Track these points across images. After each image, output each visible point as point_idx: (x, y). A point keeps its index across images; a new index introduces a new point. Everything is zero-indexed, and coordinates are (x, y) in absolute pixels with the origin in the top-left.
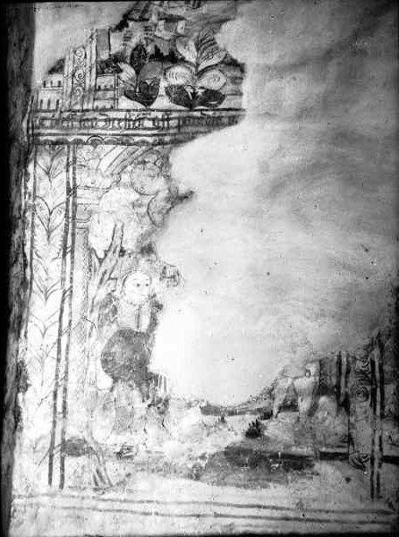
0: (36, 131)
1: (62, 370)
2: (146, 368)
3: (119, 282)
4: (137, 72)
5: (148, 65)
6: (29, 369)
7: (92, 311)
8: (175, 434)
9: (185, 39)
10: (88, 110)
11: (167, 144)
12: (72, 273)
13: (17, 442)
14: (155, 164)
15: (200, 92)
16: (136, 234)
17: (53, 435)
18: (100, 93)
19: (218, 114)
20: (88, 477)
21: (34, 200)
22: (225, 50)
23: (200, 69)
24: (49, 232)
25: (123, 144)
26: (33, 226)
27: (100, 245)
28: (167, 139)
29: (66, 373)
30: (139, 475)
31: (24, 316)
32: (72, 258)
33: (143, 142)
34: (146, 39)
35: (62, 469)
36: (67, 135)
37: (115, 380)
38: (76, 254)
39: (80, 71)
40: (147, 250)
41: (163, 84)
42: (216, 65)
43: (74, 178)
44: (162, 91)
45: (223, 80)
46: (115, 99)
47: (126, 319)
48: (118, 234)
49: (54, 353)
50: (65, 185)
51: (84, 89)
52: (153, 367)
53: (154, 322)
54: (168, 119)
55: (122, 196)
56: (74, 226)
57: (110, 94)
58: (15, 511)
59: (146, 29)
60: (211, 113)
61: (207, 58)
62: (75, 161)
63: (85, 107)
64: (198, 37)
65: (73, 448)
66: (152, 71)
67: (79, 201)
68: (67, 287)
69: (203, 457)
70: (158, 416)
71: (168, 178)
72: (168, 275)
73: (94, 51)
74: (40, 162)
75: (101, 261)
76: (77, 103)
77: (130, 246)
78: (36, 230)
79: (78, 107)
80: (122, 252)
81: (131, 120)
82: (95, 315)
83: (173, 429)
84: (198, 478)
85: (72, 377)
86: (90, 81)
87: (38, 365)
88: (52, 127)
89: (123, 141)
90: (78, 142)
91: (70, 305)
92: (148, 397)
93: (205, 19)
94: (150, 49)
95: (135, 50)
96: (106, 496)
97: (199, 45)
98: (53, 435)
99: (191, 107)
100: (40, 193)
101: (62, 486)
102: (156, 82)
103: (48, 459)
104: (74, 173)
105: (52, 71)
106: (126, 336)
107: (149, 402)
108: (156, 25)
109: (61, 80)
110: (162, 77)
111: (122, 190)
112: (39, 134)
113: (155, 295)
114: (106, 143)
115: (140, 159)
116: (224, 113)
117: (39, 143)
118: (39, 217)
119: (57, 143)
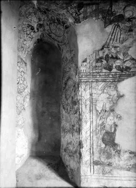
0: (80, 79)
1: (92, 142)
2: (114, 142)
3: (105, 119)
4: (107, 62)
5: (110, 60)
6: (83, 142)
7: (98, 127)
8: (123, 159)
9: (120, 53)
10: (94, 73)
11: (116, 82)
12: (92, 117)
13: (81, 161)
14: (113, 87)
15: (124, 67)
16: (109, 106)
17: (91, 160)
18: (97, 68)
19: (129, 73)
20: (101, 171)
21: (81, 97)
22: (131, 55)
23: (124, 61)
24: (86, 106)
25: (104, 82)
26: (82, 104)
27: (99, 109)
28: (116, 80)
29: (93, 143)
30: (114, 170)
31: (81, 129)
32: (92, 113)
33: (110, 81)
34: (109, 53)
35: (94, 169)
36: (89, 79)
37: (106, 145)
38: (93, 112)
39: (91, 62)
40: (112, 110)
41: (114, 65)
42: (129, 60)
43: (92, 91)
44: (114, 67)
45: (131, 64)
46: (101, 69)
47: (108, 128)
48: (104, 106)
49: (89, 138)
50: (89, 93)
51: (92, 66)
52: (116, 142)
53: (115, 130)
54: (116, 75)
55: (104, 96)
56: (92, 104)
57: (100, 68)
58: (46, 168)
59: (109, 50)
60: (127, 73)
61: (126, 58)
62: (92, 87)
63: (93, 72)
64: (123, 52)
65: (96, 163)
66: (111, 62)
67: (93, 97)
68: (91, 120)
69: (130, 165)
70: (118, 155)
71: (117, 91)
72: (118, 117)
73: (95, 56)
74: (82, 87)
75: (100, 113)
76: (91, 71)
77: (108, 109)
78: (83, 106)
79: (91, 72)
80: (106, 111)
81: (106, 75)
82: (99, 128)
83: (122, 158)
84: (129, 170)
85: (95, 145)
86: (94, 64)
87: (85, 141)
88: (85, 78)
89: (104, 81)
90: (92, 82)
91: (93, 125)
92: (115, 150)
93: (125, 47)
94: (110, 56)
95: (106, 56)
96: (106, 175)
97: (124, 54)
98: (91, 160)
99: (122, 71)
100: (83, 95)
101: (94, 173)
102: (112, 65)
103: (90, 166)
104: (92, 90)
105: (84, 62)
106: (107, 133)
107: (116, 151)
108: (112, 49)
109: (86, 64)
110: (114, 63)
111: (105, 94)
112: (81, 79)
113: (115, 123)
114: (100, 82)
115: (109, 86)
116: (131, 73)
117: (81, 82)
118: (83, 102)
119: (86, 82)
